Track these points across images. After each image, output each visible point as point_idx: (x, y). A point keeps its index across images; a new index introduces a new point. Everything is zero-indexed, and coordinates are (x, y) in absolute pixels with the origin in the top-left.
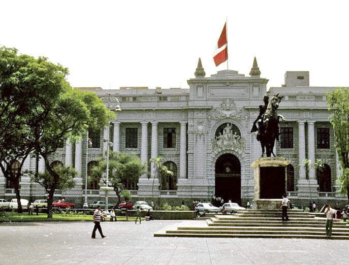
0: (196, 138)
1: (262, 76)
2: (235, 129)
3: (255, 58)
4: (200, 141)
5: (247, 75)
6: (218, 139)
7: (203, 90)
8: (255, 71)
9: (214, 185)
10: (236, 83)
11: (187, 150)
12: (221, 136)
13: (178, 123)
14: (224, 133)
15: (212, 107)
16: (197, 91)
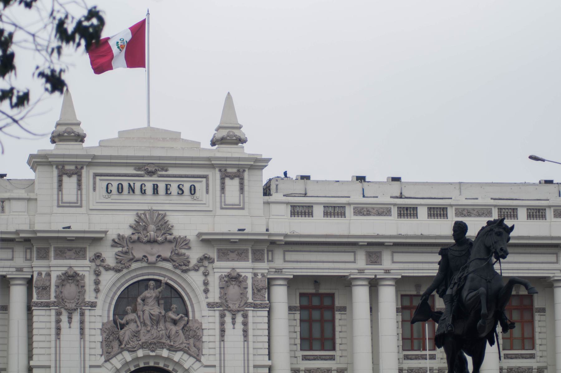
0: (58, 321)
1: (249, 149)
3: (229, 97)
4: (70, 333)
5: (206, 144)
6: (122, 326)
8: (230, 137)
11: (30, 357)
12: (132, 316)
14: (139, 308)
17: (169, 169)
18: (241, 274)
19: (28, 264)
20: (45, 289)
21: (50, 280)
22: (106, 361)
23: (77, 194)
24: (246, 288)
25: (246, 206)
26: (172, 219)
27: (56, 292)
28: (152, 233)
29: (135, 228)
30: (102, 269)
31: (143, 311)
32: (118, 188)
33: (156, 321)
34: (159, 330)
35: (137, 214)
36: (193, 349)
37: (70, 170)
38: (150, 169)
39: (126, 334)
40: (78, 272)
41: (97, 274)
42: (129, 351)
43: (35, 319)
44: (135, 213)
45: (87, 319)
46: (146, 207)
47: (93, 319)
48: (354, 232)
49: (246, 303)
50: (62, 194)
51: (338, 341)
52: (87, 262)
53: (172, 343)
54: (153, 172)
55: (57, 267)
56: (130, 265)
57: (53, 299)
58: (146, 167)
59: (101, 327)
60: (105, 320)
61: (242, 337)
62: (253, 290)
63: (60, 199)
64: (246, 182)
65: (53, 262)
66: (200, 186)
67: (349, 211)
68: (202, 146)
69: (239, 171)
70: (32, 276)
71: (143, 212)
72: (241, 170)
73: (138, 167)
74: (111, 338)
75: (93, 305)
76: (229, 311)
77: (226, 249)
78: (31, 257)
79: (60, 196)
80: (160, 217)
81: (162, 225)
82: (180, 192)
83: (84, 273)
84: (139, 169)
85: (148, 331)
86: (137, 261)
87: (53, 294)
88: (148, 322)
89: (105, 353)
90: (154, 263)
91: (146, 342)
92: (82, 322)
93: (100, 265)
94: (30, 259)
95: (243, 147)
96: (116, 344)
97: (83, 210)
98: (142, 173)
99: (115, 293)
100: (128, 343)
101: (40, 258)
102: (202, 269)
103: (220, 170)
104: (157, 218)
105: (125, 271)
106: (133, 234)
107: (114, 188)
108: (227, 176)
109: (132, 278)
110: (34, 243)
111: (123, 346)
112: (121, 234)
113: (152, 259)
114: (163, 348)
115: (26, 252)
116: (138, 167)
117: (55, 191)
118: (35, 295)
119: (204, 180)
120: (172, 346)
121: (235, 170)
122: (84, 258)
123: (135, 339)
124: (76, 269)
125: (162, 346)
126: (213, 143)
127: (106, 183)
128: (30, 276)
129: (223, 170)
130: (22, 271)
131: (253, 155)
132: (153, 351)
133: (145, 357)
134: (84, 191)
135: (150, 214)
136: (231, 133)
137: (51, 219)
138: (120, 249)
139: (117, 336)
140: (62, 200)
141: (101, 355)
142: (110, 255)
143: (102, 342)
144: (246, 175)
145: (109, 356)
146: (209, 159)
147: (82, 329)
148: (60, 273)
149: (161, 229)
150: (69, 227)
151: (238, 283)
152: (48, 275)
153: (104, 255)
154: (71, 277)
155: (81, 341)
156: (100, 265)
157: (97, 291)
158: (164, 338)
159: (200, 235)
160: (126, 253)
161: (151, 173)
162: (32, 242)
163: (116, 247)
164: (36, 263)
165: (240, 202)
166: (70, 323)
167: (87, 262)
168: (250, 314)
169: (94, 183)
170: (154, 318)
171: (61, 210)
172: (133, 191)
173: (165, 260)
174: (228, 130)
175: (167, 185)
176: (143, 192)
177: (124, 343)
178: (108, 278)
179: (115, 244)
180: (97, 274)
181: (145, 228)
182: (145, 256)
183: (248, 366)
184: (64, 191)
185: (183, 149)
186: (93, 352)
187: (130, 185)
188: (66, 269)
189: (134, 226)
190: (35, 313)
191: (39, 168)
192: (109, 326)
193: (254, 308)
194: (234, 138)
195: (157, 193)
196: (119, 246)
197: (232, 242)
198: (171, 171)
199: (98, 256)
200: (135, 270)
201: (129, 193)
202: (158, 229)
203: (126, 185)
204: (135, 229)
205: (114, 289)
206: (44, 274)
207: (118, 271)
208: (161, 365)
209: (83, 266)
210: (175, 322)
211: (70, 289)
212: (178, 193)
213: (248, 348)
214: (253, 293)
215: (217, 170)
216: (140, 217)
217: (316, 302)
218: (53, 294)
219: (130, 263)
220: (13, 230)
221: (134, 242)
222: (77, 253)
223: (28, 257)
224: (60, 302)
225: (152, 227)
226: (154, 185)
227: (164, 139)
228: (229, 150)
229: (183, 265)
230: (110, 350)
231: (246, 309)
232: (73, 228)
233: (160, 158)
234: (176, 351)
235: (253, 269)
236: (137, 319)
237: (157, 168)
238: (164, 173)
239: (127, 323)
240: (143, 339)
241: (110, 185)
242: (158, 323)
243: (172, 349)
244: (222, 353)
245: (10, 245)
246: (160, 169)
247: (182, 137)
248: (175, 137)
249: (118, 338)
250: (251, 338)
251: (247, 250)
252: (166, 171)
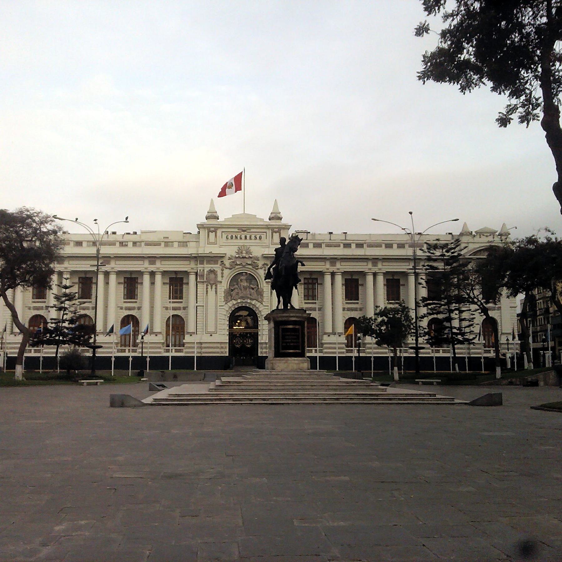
0: (207, 289)
1: (283, 222)
2: (252, 278)
4: (212, 293)
6: (232, 290)
7: (216, 236)
8: (276, 217)
9: (228, 341)
10: (254, 228)
16: (208, 236)
19: (196, 266)
20: (202, 276)
26: (252, 249)
33: (245, 288)
36: (260, 300)
41: (222, 270)
46: (242, 244)
48: (325, 254)
52: (218, 266)
57: (205, 280)
65: (205, 265)
66: (263, 236)
67: (323, 246)
73: (239, 228)
75: (221, 282)
92: (216, 289)
94: (197, 265)
96: (229, 298)
101: (200, 264)
102: (264, 268)
110: (198, 258)
113: (244, 264)
116: (239, 228)
122: (217, 264)
125: (248, 298)
142: (227, 263)
145: (227, 302)
146: (267, 225)
159: (263, 255)
160: (233, 262)
164: (199, 266)
173: (249, 265)
176: (241, 238)
179: (230, 259)
180: (222, 270)
181: (242, 253)
198: (252, 230)
202: (247, 253)
203: (234, 236)
207: (230, 269)
209: (217, 267)
210: (253, 289)
217: (310, 281)
221: (237, 258)
229: (256, 267)
233: (247, 225)
239: (234, 289)
240: (240, 295)
243: (251, 299)
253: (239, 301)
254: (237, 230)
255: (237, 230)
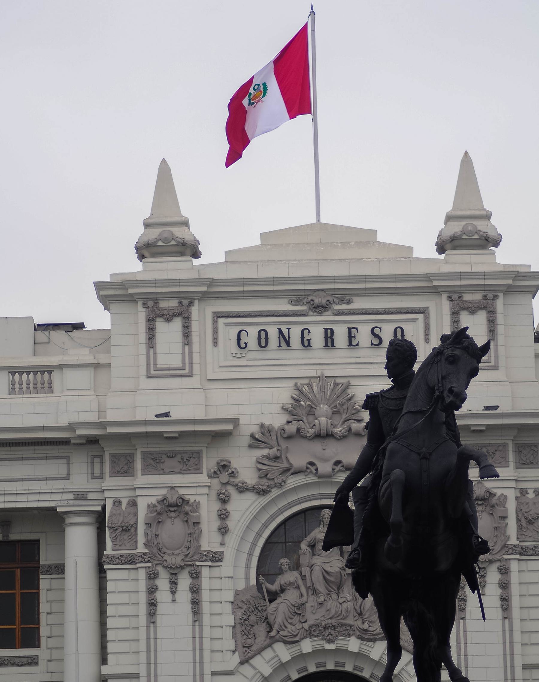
0: (152, 590)
1: (504, 256)
3: (467, 162)
4: (174, 611)
5: (426, 250)
6: (273, 596)
11: (104, 661)
13: (53, 510)
14: (304, 560)
15: (235, 422)
17: (355, 299)
18: (494, 491)
19: (95, 484)
20: (128, 530)
21: (136, 514)
22: (242, 663)
23: (184, 353)
24: (504, 518)
25: (502, 362)
27: (146, 535)
28: (323, 420)
29: (293, 411)
30: (231, 490)
31: (311, 567)
32: (259, 338)
34: (341, 600)
35: (296, 384)
37: (170, 309)
38: (317, 301)
39: (279, 610)
40: (187, 497)
41: (224, 500)
42: (286, 643)
43: (110, 587)
44: (291, 383)
45: (205, 583)
47: (217, 584)
49: (504, 546)
50: (155, 354)
51: (44, 631)
52: (203, 478)
53: (366, 626)
54: (323, 307)
55: (147, 488)
56: (284, 482)
57: (141, 549)
58: (310, 298)
59: (232, 599)
60: (241, 586)
61: (500, 610)
62: (518, 520)
63: (152, 362)
64: (500, 319)
65: (141, 479)
68: (417, 254)
69: (485, 297)
70: (104, 507)
71: (306, 381)
72: (490, 296)
73: (296, 298)
74: (253, 618)
75: (216, 558)
76: (165, 567)
77: (160, 453)
78: (102, 473)
79: (152, 357)
80: (339, 388)
81: (342, 404)
82: (376, 341)
83: (198, 498)
84: (298, 302)
85: (321, 604)
86: (297, 472)
87: (141, 540)
88: (321, 587)
89: (240, 646)
90: (330, 476)
91: (317, 625)
92: (195, 590)
93: (227, 483)
94: (101, 477)
95: (494, 253)
96: (261, 630)
97: (194, 381)
98: (304, 308)
99: (259, 535)
100: (283, 627)
101: (115, 473)
103: (450, 298)
104: (333, 390)
105: (275, 492)
106: (288, 422)
107: (251, 338)
108: (463, 309)
109: (290, 506)
110: (103, 446)
111: (273, 634)
112: (267, 423)
113: (325, 468)
114: (349, 635)
115: (93, 463)
116: (296, 298)
117: (143, 349)
118: (109, 543)
119: (421, 317)
120: (365, 630)
121: (478, 297)
122: (198, 470)
123: (296, 618)
124: (182, 491)
125: (348, 631)
126: (441, 248)
127: (237, 329)
128: (99, 508)
129: (455, 296)
130: (86, 499)
131: (513, 266)
132: (330, 641)
133: (315, 653)
134: (196, 347)
135: (320, 386)
136: (470, 228)
137: (135, 401)
138: (266, 452)
139: (264, 614)
140: (155, 364)
141: (234, 652)
142: (245, 464)
143: (234, 627)
144: (500, 304)
145: (247, 654)
146: (428, 277)
147: (196, 603)
148: (153, 500)
149: (342, 411)
150: (167, 415)
151: (488, 508)
152: (133, 504)
153: (235, 464)
154: (175, 507)
155: (194, 626)
156: (227, 483)
157: (224, 531)
158: (351, 616)
160: (276, 458)
161: (320, 309)
162: (102, 443)
163: (258, 447)
164: (110, 482)
165: (184, 364)
166: (173, 592)
167: (203, 478)
168: (514, 566)
169: (215, 331)
170: (332, 579)
171: (154, 383)
172: (288, 343)
174: (463, 223)
175: (350, 329)
176: (306, 344)
177: (276, 627)
178: (243, 507)
179: (256, 442)
180: (224, 500)
181: (311, 412)
182: (312, 464)
183: (513, 667)
184: (160, 348)
185: (379, 260)
186: (217, 645)
187: (280, 332)
188: (164, 492)
189: (290, 408)
190: (110, 575)
191: (113, 306)
192: (248, 597)
193: (521, 554)
194: (476, 236)
195: (333, 345)
196: (263, 445)
197: (474, 431)
198: (359, 304)
199: (224, 467)
200: (295, 489)
201: (280, 346)
202: (336, 413)
203: (273, 332)
204: (291, 413)
205: (257, 527)
206: (124, 502)
207: (262, 492)
208: (349, 668)
209: (195, 486)
211: (173, 530)
212: (372, 344)
213: (511, 631)
214: (520, 527)
215: (444, 297)
216: (300, 391)
218: (141, 540)
219: (284, 478)
220: (64, 421)
221: (290, 437)
222: (183, 461)
223: (97, 472)
224: (155, 555)
225: (323, 409)
226: (326, 330)
227: (344, 244)
228: (467, 259)
230: (249, 641)
231: (506, 557)
232: (174, 416)
233: (335, 279)
234: (374, 640)
235: (516, 481)
236: (300, 582)
237: (330, 299)
238: (344, 307)
239: (283, 591)
240: (312, 619)
241: (243, 333)
242: (340, 587)
244: (462, 642)
245: (63, 450)
246: (336, 300)
247: (380, 238)
248: (366, 238)
249: (266, 618)
250: (516, 613)
251: (505, 445)
252: (349, 302)
253: (307, 646)
254: (283, 305)
255: (283, 305)
